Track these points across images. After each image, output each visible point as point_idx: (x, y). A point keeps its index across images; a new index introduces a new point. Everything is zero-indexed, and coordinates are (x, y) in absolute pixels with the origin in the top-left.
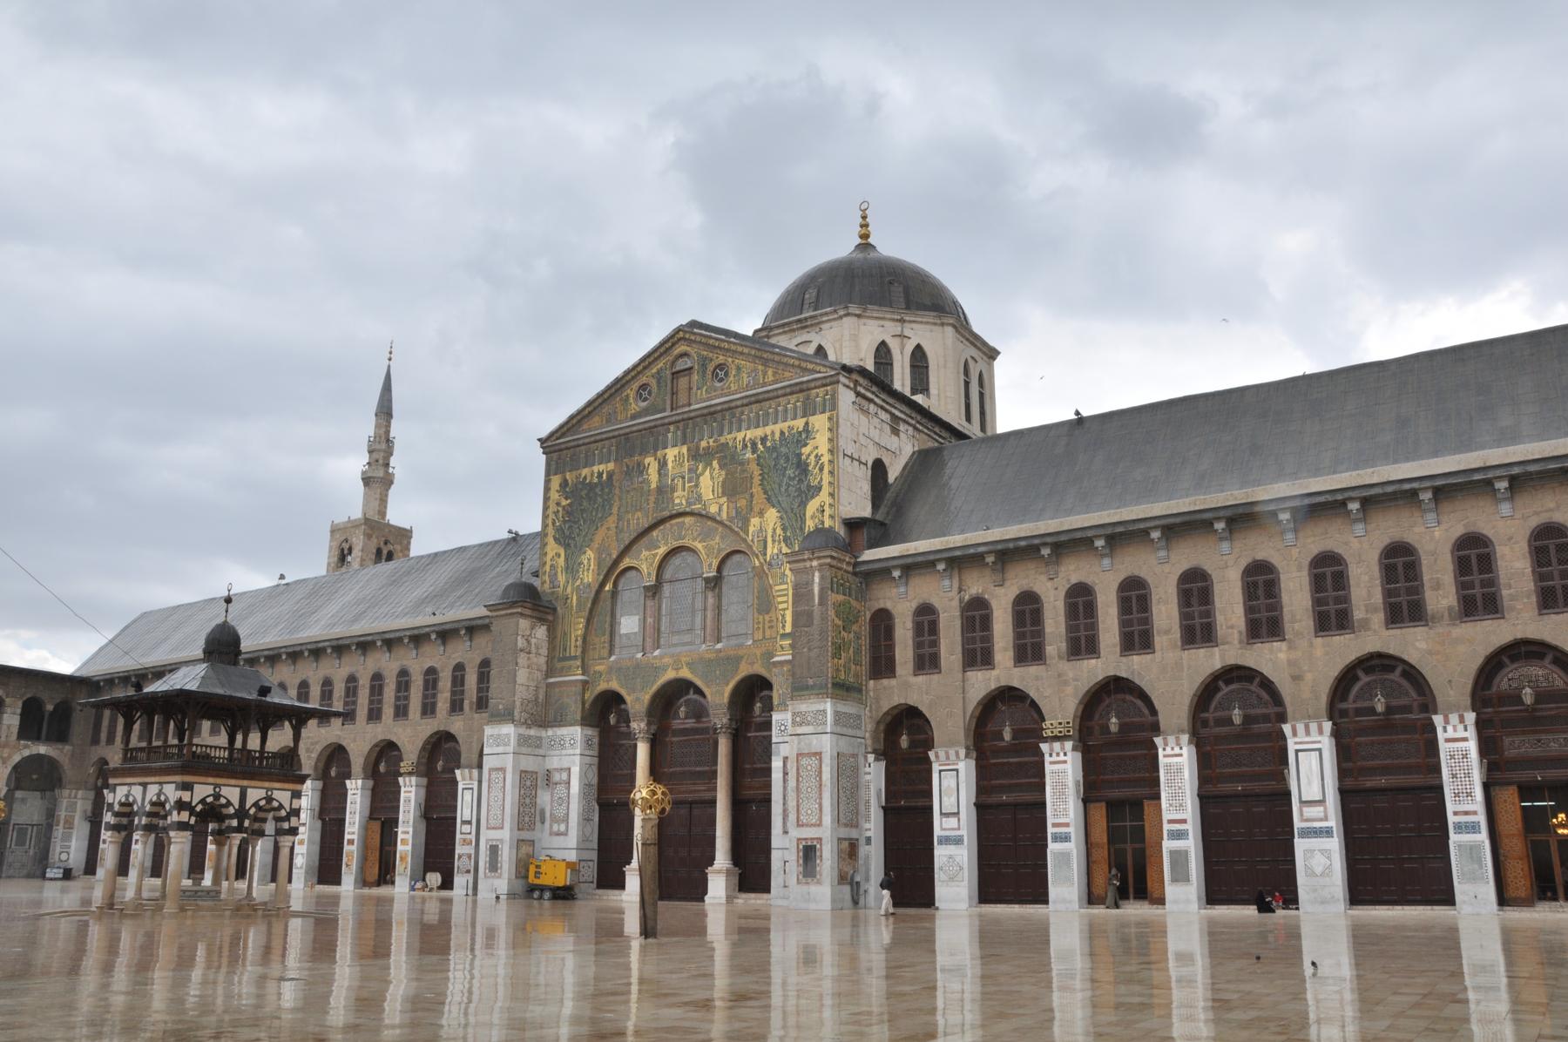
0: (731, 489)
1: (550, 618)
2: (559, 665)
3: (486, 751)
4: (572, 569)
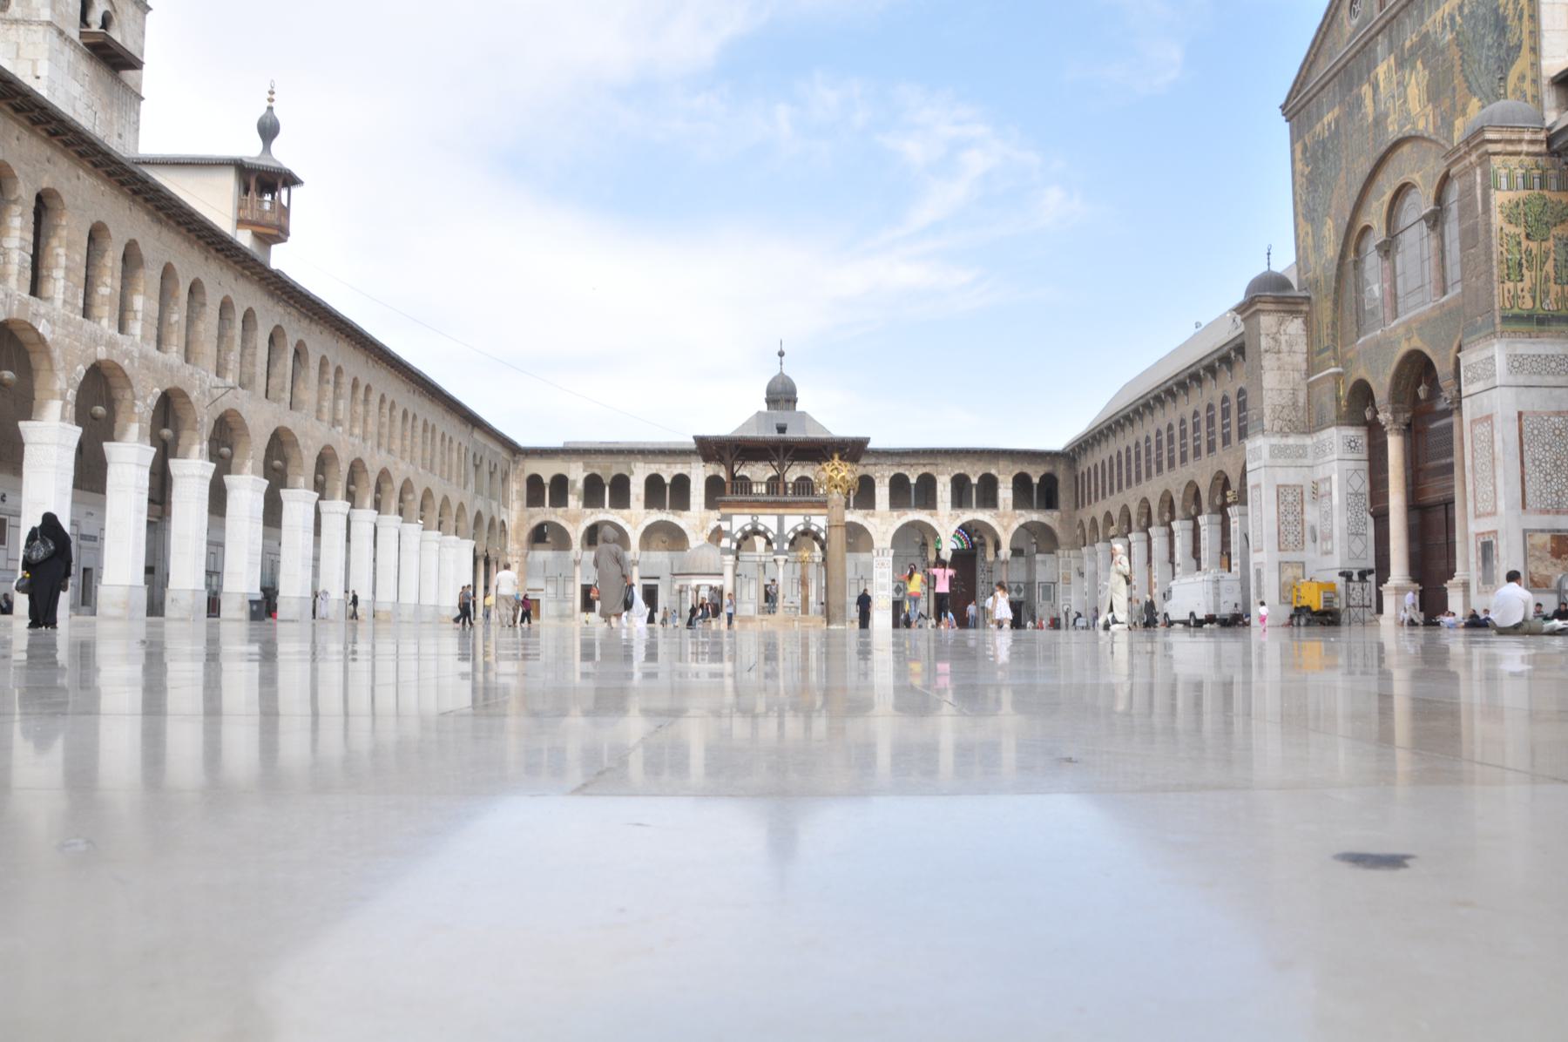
0: (1434, 94)
1: (1305, 308)
2: (1317, 360)
3: (1249, 467)
4: (1317, 248)
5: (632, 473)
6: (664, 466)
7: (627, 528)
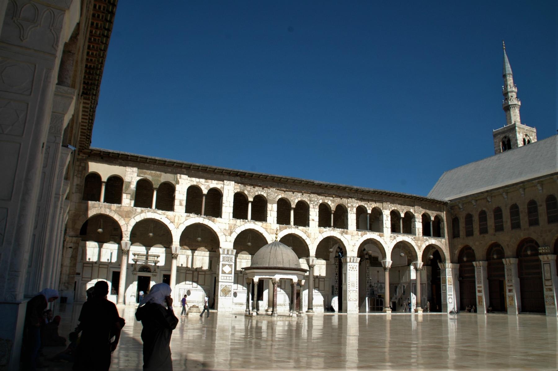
5: (178, 182)
6: (202, 181)
7: (171, 227)
